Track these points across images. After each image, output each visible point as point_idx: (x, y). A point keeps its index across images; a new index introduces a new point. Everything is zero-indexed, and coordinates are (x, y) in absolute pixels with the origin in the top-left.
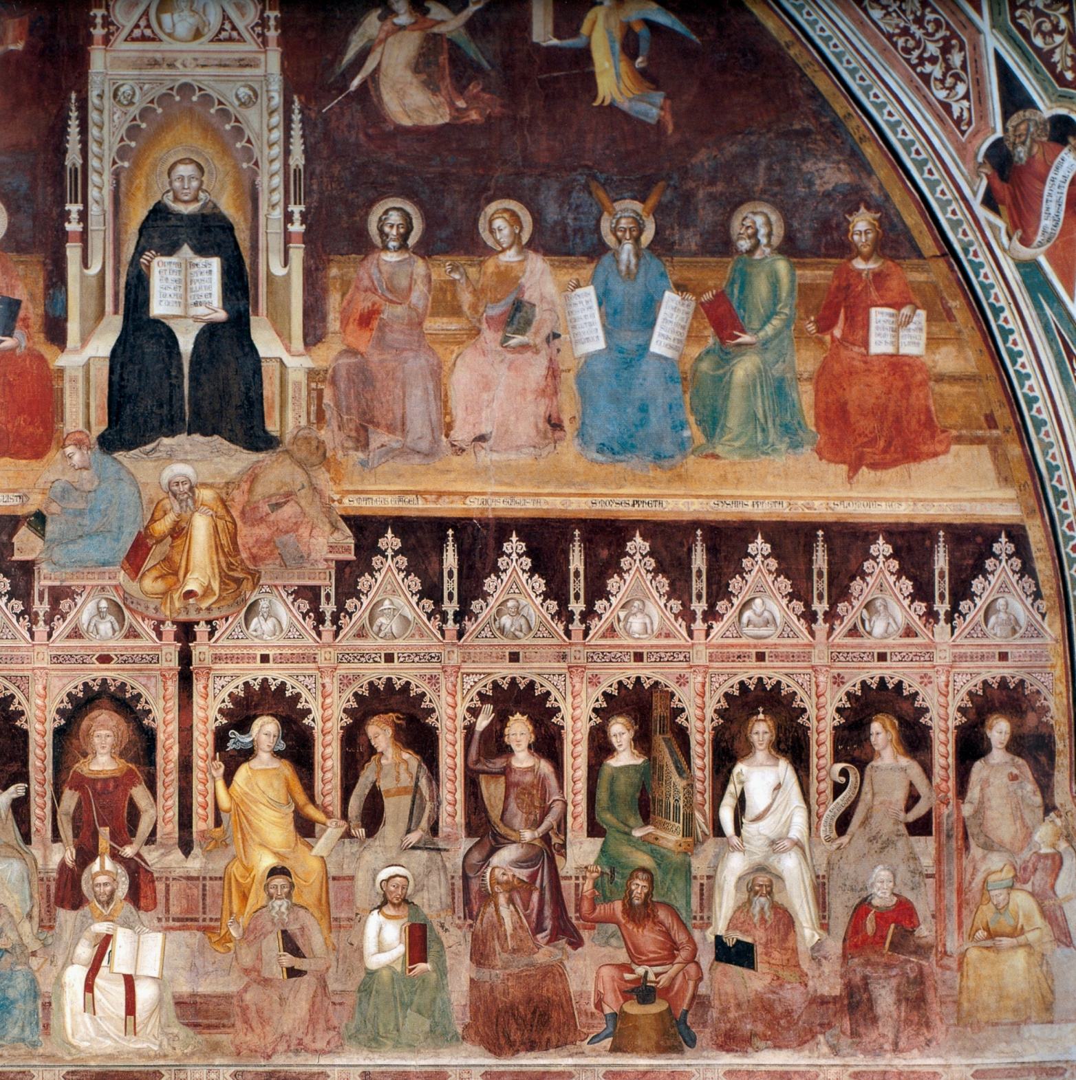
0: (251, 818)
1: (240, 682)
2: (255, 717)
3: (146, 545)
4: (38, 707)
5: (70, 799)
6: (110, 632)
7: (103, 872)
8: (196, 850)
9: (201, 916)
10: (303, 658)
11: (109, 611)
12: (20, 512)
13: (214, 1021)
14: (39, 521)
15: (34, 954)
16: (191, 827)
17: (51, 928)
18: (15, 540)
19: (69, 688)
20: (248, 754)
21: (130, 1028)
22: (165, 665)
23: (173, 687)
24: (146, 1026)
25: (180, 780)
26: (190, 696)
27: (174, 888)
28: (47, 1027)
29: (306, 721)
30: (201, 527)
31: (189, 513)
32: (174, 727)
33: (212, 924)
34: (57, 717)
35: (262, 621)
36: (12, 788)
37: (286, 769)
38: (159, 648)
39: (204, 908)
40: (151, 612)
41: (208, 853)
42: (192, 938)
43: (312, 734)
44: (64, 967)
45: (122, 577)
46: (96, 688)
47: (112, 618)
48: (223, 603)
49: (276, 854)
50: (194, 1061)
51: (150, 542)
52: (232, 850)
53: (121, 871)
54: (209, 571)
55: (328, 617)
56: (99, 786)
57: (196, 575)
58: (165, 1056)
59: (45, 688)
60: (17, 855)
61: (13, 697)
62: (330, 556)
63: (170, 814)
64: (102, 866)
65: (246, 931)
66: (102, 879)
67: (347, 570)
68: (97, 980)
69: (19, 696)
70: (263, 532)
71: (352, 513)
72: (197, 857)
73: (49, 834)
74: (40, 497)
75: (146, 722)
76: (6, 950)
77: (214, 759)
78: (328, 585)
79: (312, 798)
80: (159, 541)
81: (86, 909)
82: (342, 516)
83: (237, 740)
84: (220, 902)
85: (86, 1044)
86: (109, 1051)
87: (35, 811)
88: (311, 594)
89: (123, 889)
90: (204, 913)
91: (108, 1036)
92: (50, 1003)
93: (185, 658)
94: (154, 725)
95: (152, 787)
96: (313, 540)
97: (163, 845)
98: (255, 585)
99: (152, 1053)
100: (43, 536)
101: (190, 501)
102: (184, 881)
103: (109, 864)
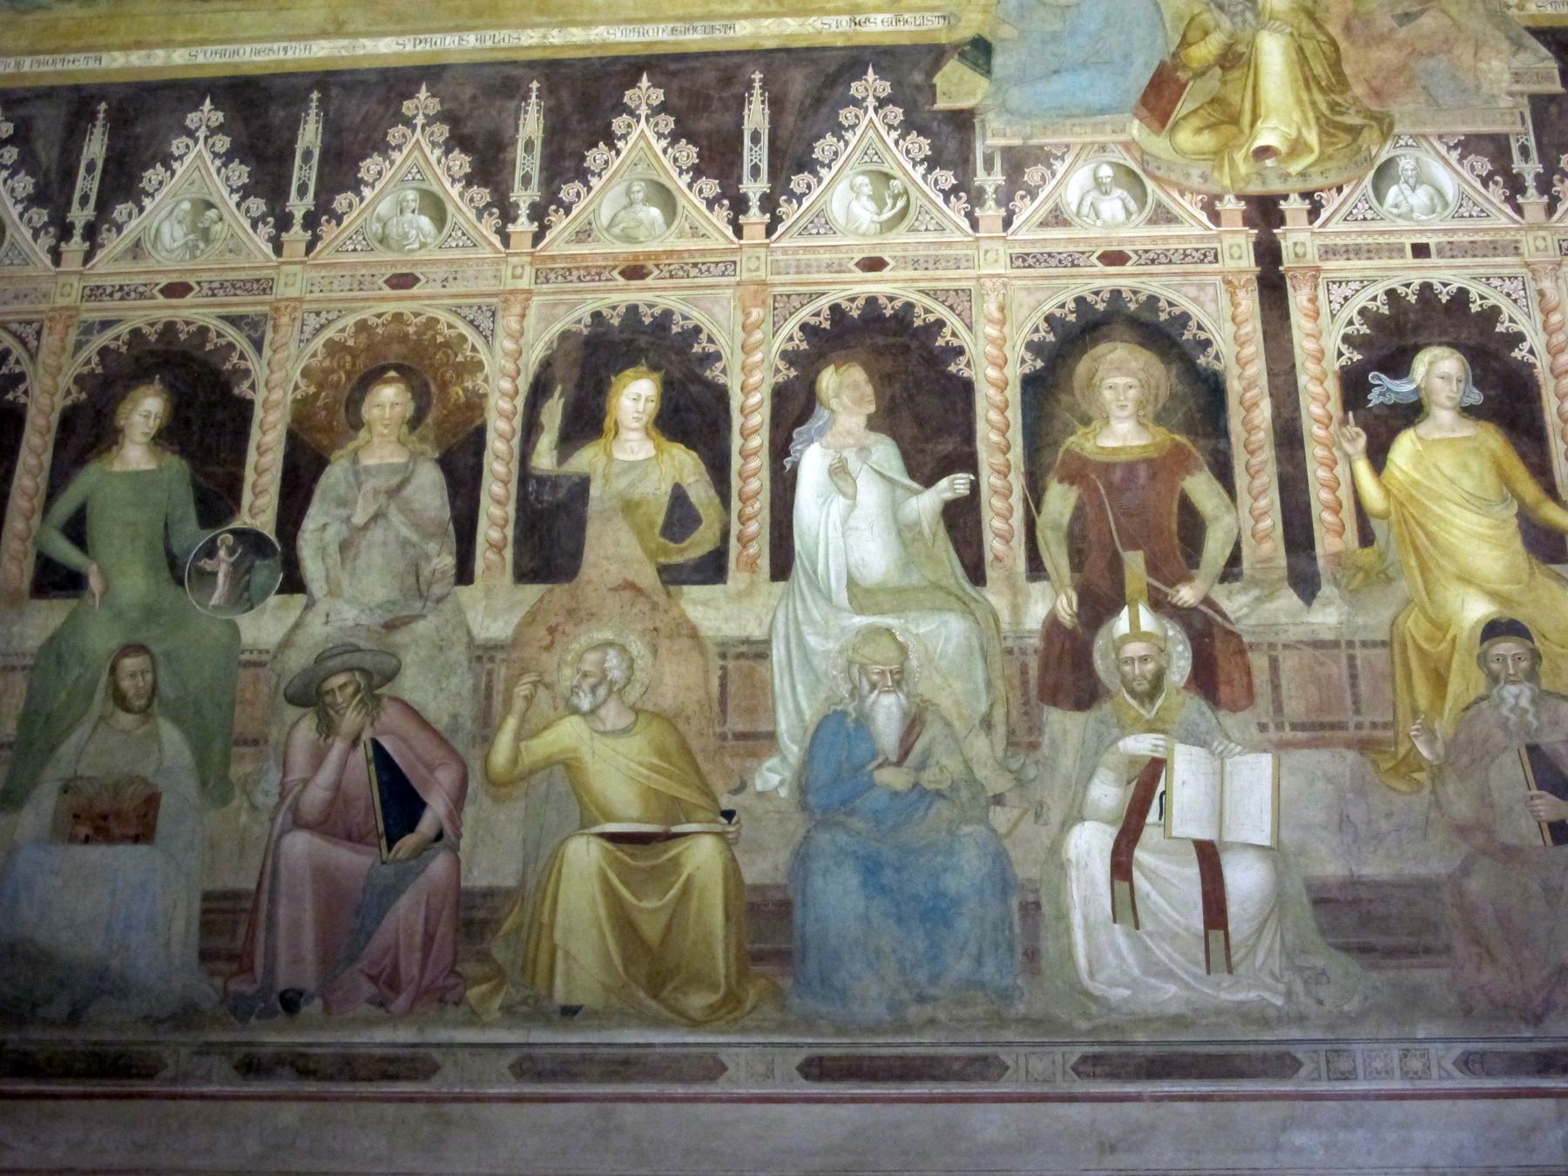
0: (1433, 528)
1: (1379, 289)
2: (1417, 349)
3: (1177, 81)
4: (992, 341)
5: (1060, 501)
6: (1121, 215)
7: (1136, 634)
8: (1327, 590)
9: (1352, 720)
10: (1494, 248)
11: (1116, 181)
12: (943, 39)
13: (1405, 940)
14: (980, 52)
15: (998, 800)
16: (1312, 547)
17: (1034, 746)
18: (938, 80)
19: (1049, 307)
20: (1412, 412)
21: (1218, 956)
22: (1228, 264)
23: (1249, 301)
24: (1252, 950)
25: (1279, 461)
26: (1286, 316)
27: (1288, 662)
28: (1032, 955)
29: (1517, 354)
30: (1273, 53)
31: (1249, 31)
32: (1258, 368)
33: (1379, 734)
34: (1028, 356)
35: (1408, 192)
36: (944, 483)
37: (1491, 439)
38: (1218, 237)
39: (1356, 702)
40: (1196, 181)
41: (1353, 596)
42: (1339, 763)
43: (1532, 377)
44: (1066, 826)
45: (1136, 129)
46: (1101, 307)
47: (1119, 192)
48: (1329, 165)
49: (1493, 595)
50: (1365, 1031)
51: (1182, 75)
52: (1403, 586)
53: (1173, 631)
54: (1296, 116)
55: (1530, 182)
56: (1117, 476)
57: (1273, 122)
58: (1301, 1019)
59: (1002, 309)
60: (956, 605)
61: (941, 324)
62: (1517, 88)
63: (1266, 523)
64: (1134, 622)
65: (1452, 745)
66: (1135, 649)
67: (1553, 109)
68: (1140, 854)
69: (953, 321)
70: (1388, 55)
71: (1546, 24)
72: (1329, 602)
73: (1021, 565)
74: (980, 17)
75: (1202, 361)
76: (939, 794)
77: (1345, 422)
78: (1522, 132)
79: (1551, 491)
80: (1201, 74)
81: (1106, 707)
82: (1529, 29)
83: (1385, 390)
84: (1387, 688)
85: (1126, 993)
86: (1173, 1009)
87: (992, 523)
88: (1497, 148)
89: (1181, 665)
90: (1357, 711)
91: (1169, 975)
92: (1037, 905)
93: (1268, 254)
94: (1217, 367)
95: (1223, 472)
96: (1483, 66)
97: (1255, 582)
98: (1386, 133)
99: (1271, 1013)
100: (988, 72)
101: (1249, 15)
102: (1308, 652)
103: (1147, 620)
